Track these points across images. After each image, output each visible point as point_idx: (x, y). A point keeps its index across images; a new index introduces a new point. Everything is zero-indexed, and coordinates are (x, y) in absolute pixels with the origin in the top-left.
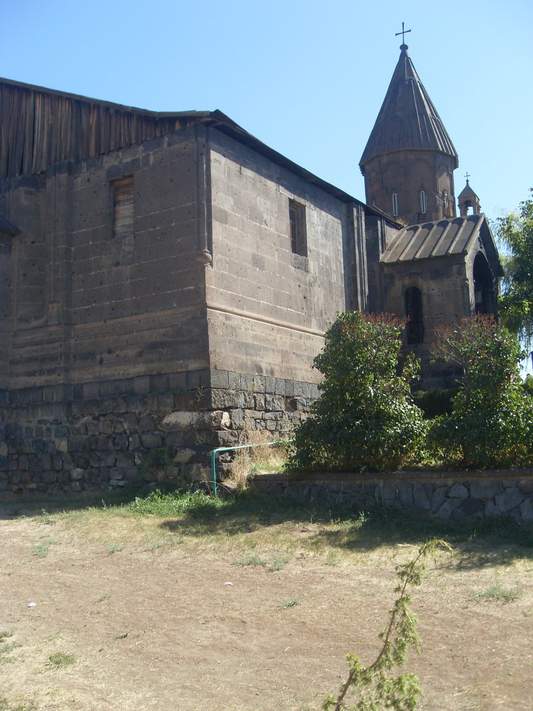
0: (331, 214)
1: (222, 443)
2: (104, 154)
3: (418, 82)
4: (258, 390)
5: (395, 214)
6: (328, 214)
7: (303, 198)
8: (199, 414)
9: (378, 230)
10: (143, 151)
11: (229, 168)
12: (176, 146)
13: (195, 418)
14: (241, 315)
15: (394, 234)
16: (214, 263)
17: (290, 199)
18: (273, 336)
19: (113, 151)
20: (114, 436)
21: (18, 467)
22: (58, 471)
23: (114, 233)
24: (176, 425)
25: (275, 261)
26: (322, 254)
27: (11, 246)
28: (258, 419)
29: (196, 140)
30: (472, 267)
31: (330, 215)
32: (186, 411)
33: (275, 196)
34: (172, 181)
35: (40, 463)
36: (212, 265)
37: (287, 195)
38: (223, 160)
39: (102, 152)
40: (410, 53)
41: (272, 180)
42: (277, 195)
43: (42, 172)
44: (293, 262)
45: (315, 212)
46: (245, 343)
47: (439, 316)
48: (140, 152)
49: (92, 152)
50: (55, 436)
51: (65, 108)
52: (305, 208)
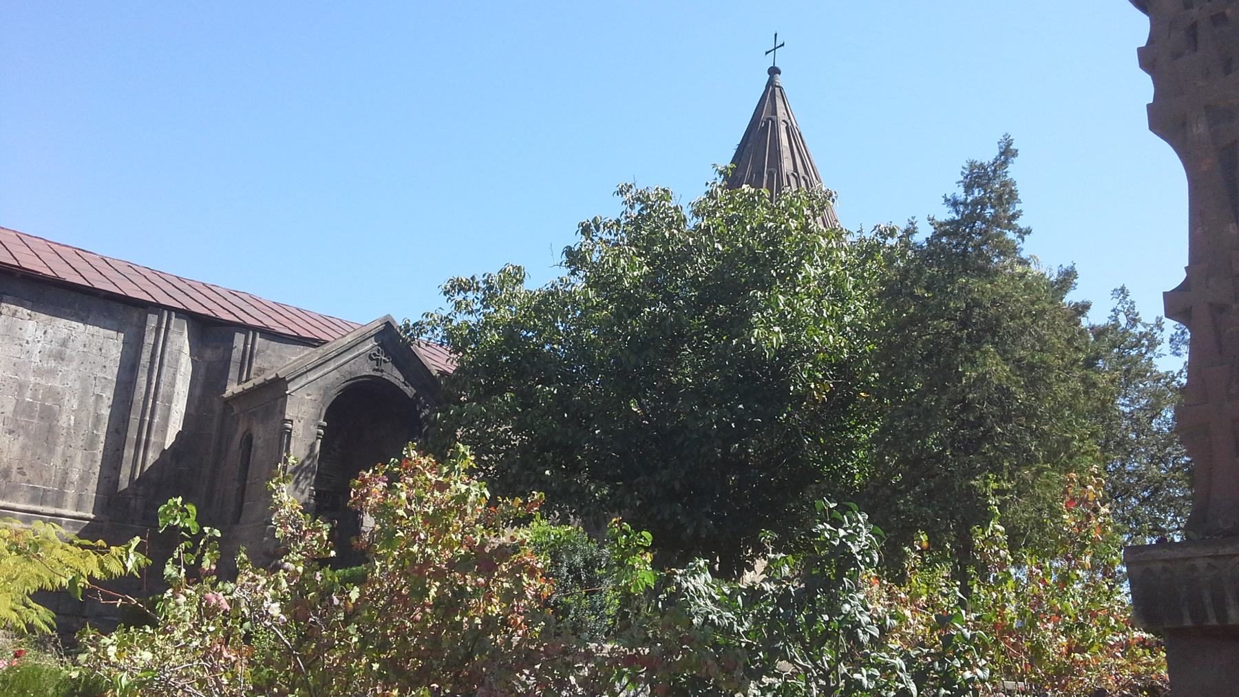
3: (784, 121)
9: (230, 349)
15: (294, 354)
40: (780, 80)
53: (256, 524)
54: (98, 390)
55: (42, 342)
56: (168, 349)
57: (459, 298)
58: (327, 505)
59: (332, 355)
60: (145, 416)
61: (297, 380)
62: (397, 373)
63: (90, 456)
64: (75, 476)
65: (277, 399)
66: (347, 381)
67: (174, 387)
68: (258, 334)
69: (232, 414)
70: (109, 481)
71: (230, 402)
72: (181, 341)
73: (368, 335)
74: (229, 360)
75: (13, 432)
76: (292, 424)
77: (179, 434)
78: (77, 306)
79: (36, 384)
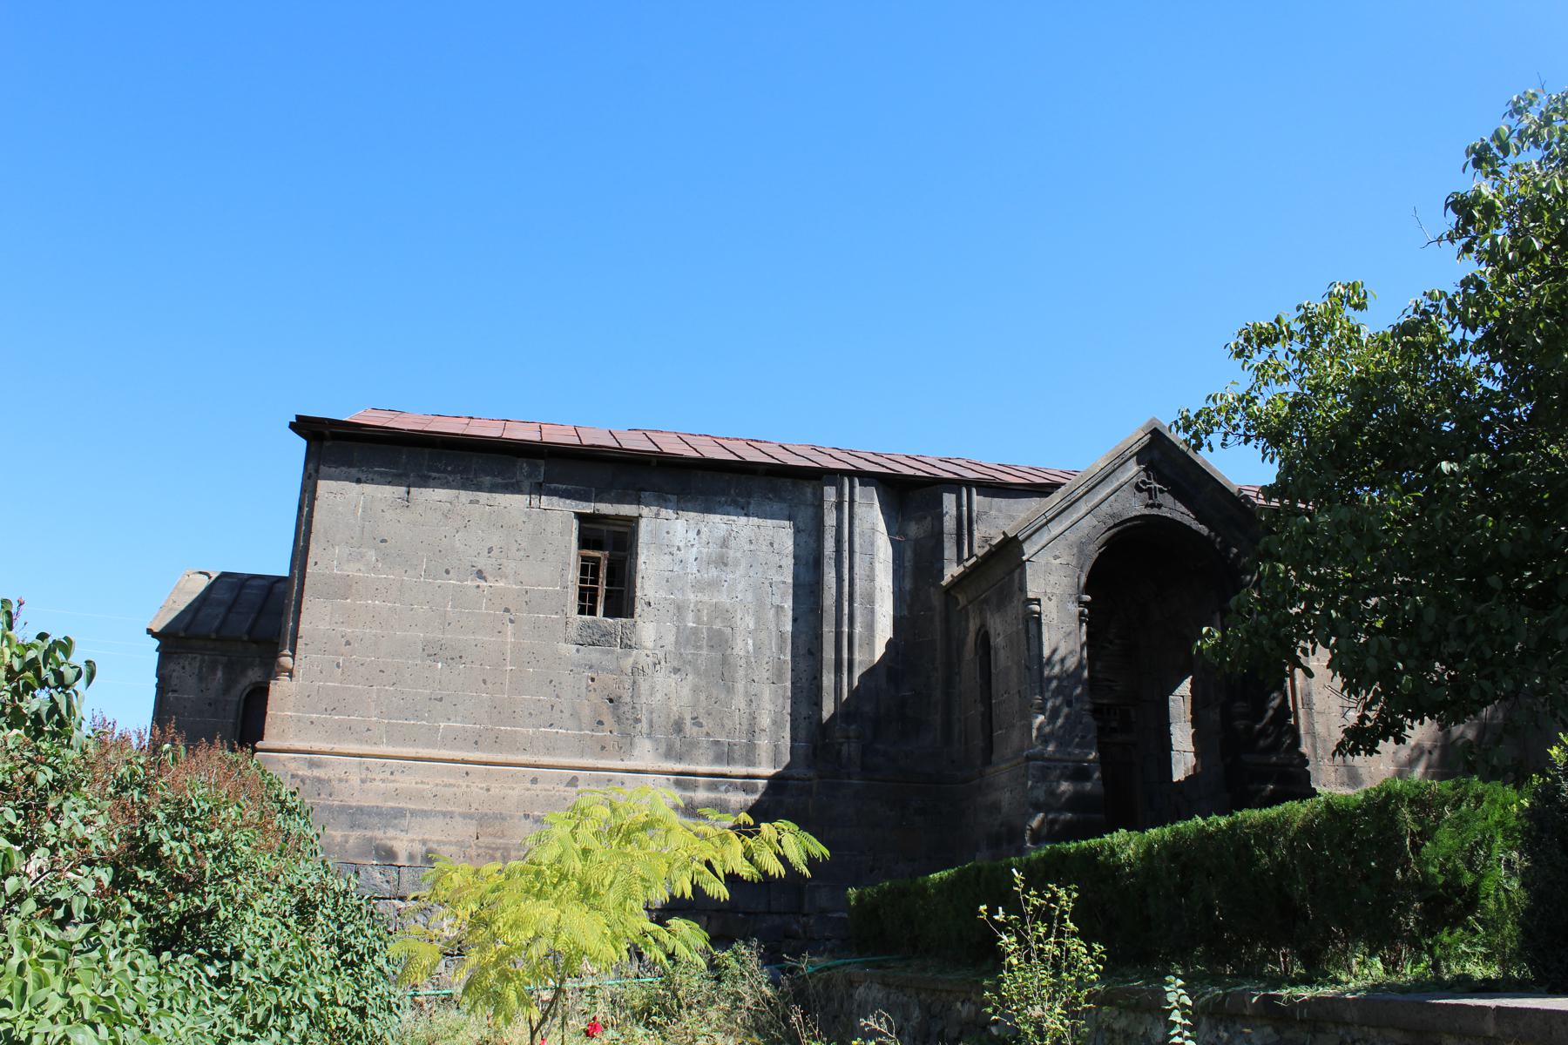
0: (746, 515)
6: (735, 518)
9: (940, 517)
16: (299, 672)
25: (505, 643)
31: (743, 519)
36: (291, 676)
38: (352, 489)
42: (529, 516)
44: (573, 632)
52: (637, 523)
53: (1015, 762)
54: (777, 600)
55: (697, 546)
56: (857, 530)
57: (1259, 358)
58: (1114, 724)
59: (1080, 491)
60: (842, 627)
61: (1035, 537)
63: (780, 692)
64: (765, 721)
65: (1013, 571)
66: (1109, 529)
67: (873, 580)
68: (974, 491)
69: (959, 607)
70: (811, 723)
71: (952, 593)
72: (871, 516)
73: (1128, 454)
74: (941, 532)
75: (679, 670)
76: (1039, 605)
77: (889, 644)
78: (732, 492)
79: (697, 603)
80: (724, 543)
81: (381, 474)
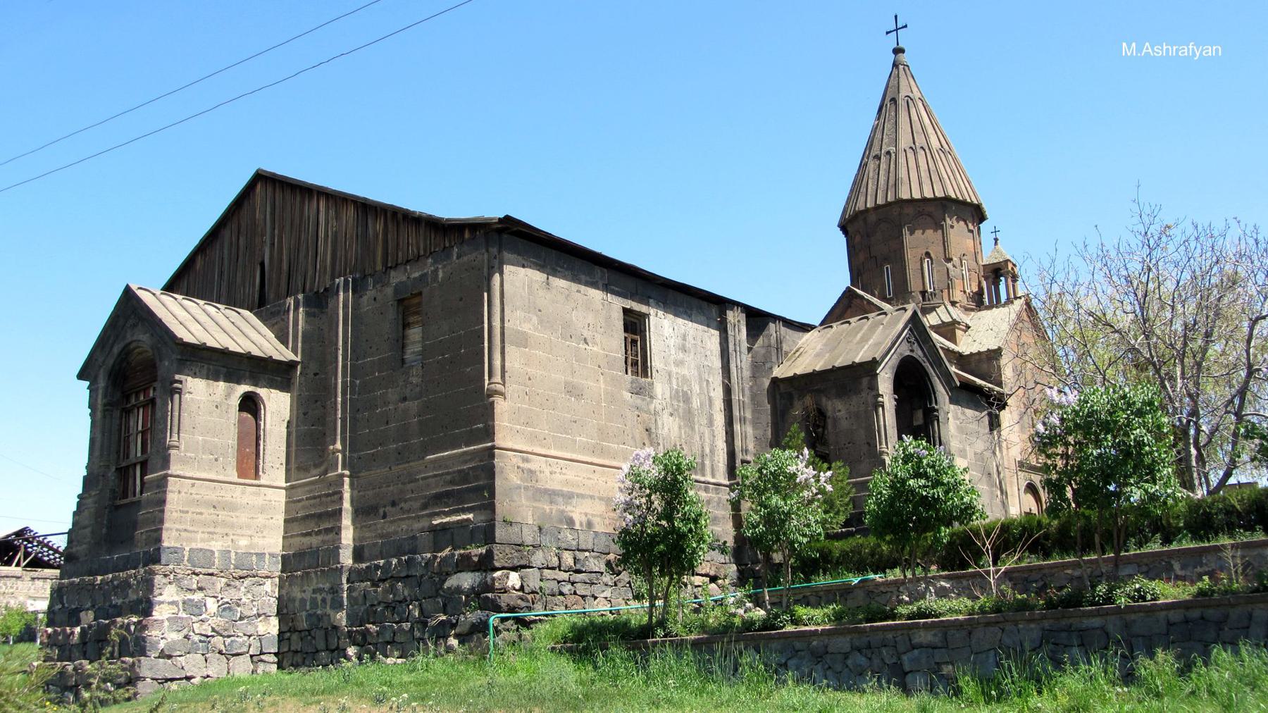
1: (506, 609)
2: (391, 268)
4: (566, 547)
5: (890, 294)
6: (686, 322)
7: (646, 305)
8: (482, 574)
10: (432, 265)
11: (531, 281)
12: (465, 259)
13: (478, 580)
14: (545, 456)
16: (508, 396)
17: (624, 309)
18: (594, 480)
19: (401, 264)
20: (393, 605)
21: (290, 648)
22: (333, 651)
23: (403, 361)
24: (458, 590)
26: (677, 373)
27: (290, 379)
28: (564, 581)
29: (487, 251)
30: (892, 377)
32: (469, 571)
33: (601, 307)
34: (461, 299)
35: (314, 642)
37: (617, 304)
39: (389, 265)
41: (598, 288)
42: (604, 306)
43: (326, 290)
45: (666, 321)
46: (549, 490)
47: (847, 445)
48: (429, 265)
49: (379, 267)
50: (331, 608)
51: (350, 213)
62: (920, 353)
80: (684, 339)
81: (534, 263)
